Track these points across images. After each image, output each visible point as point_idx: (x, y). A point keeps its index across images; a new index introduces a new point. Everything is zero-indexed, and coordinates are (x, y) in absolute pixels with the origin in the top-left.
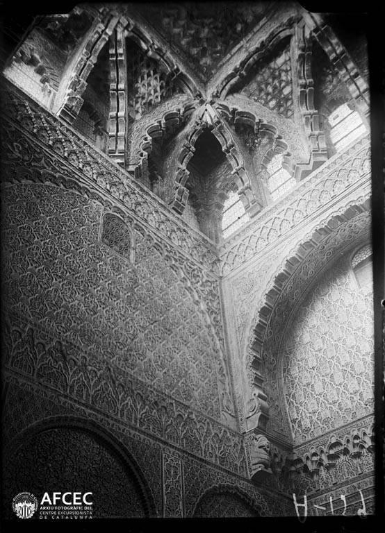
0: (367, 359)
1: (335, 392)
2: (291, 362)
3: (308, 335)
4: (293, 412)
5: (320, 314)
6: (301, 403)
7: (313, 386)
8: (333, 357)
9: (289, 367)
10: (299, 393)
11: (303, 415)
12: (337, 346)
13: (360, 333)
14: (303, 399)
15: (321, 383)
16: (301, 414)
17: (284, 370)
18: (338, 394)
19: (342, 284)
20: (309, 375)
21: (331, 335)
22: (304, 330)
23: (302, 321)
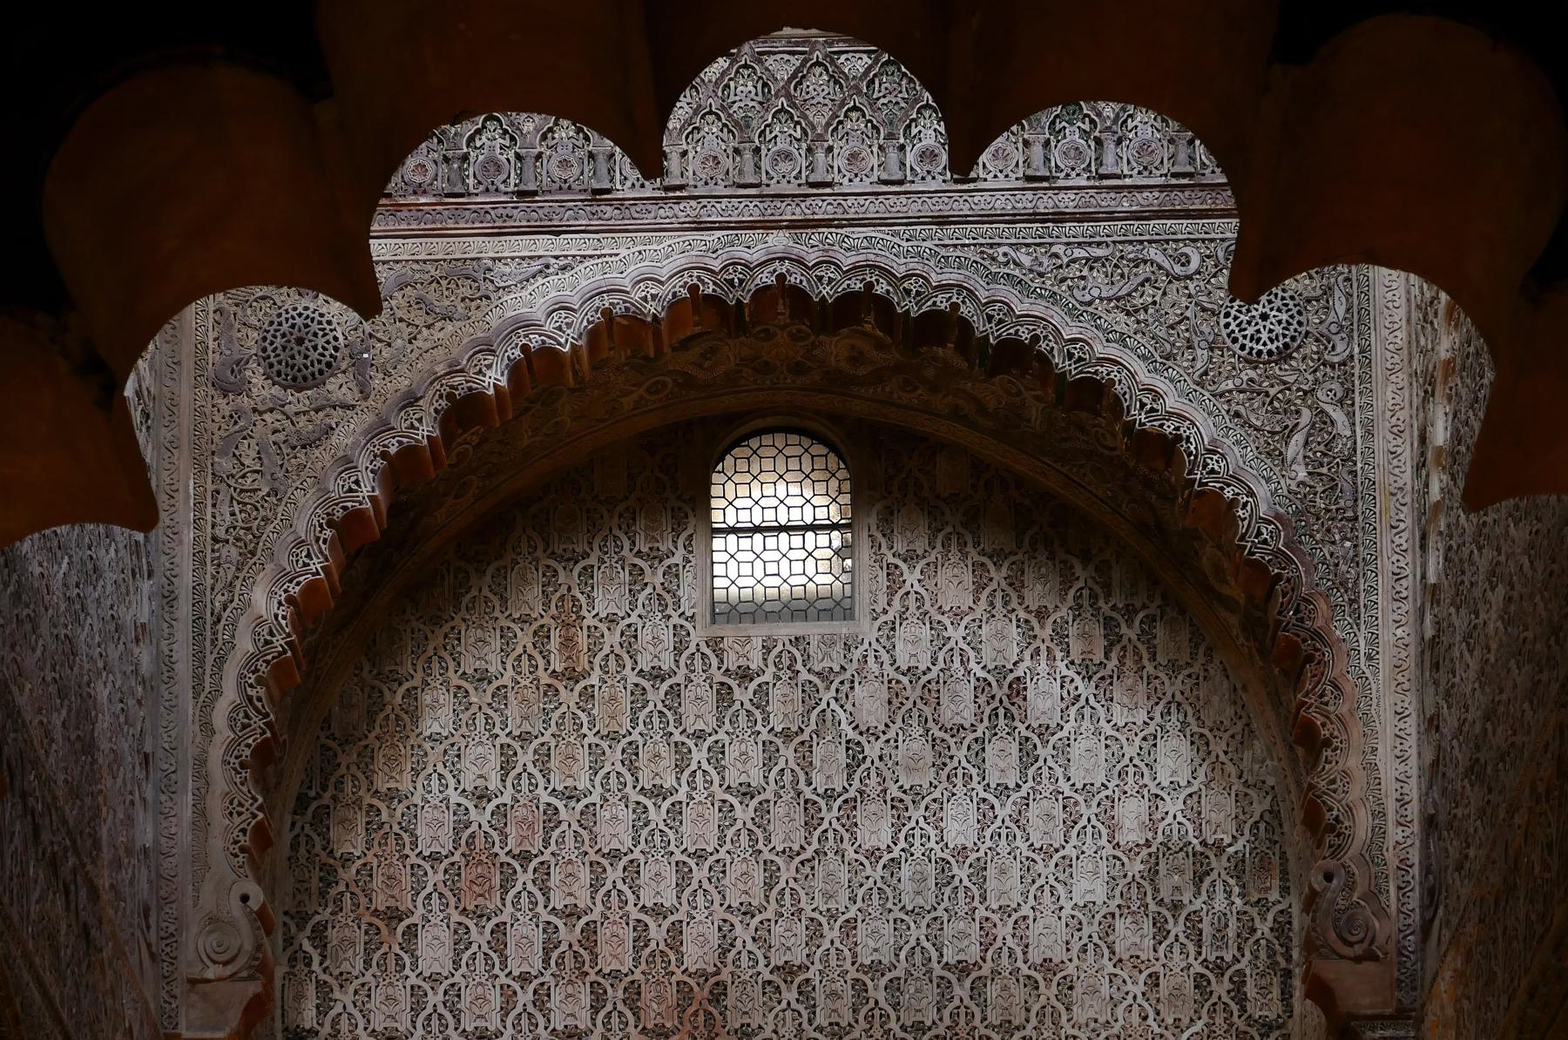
0: (653, 932)
1: (496, 999)
2: (340, 783)
3: (445, 698)
4: (299, 997)
5: (524, 638)
6: (344, 979)
7: (411, 932)
8: (525, 857)
9: (326, 798)
10: (347, 931)
11: (344, 1025)
12: (551, 818)
13: (657, 816)
14: (360, 964)
15: (446, 936)
16: (335, 1022)
17: (302, 802)
18: (505, 1011)
19: (655, 557)
20: (406, 880)
21: (543, 757)
22: (435, 666)
23: (437, 621)
